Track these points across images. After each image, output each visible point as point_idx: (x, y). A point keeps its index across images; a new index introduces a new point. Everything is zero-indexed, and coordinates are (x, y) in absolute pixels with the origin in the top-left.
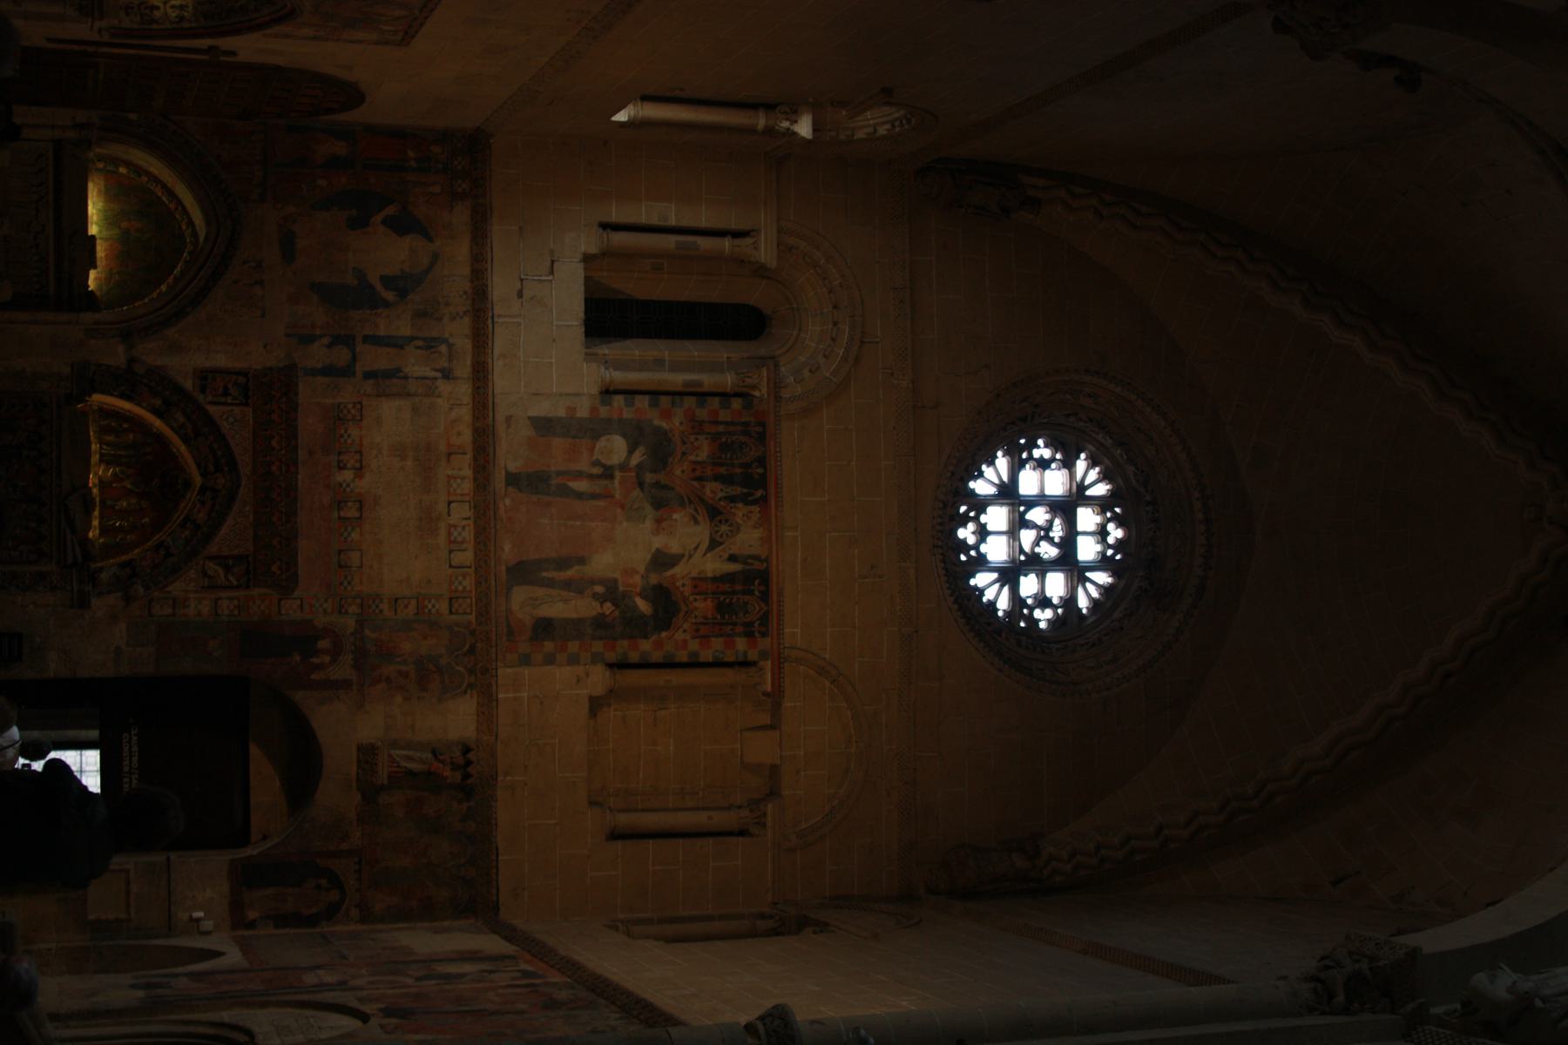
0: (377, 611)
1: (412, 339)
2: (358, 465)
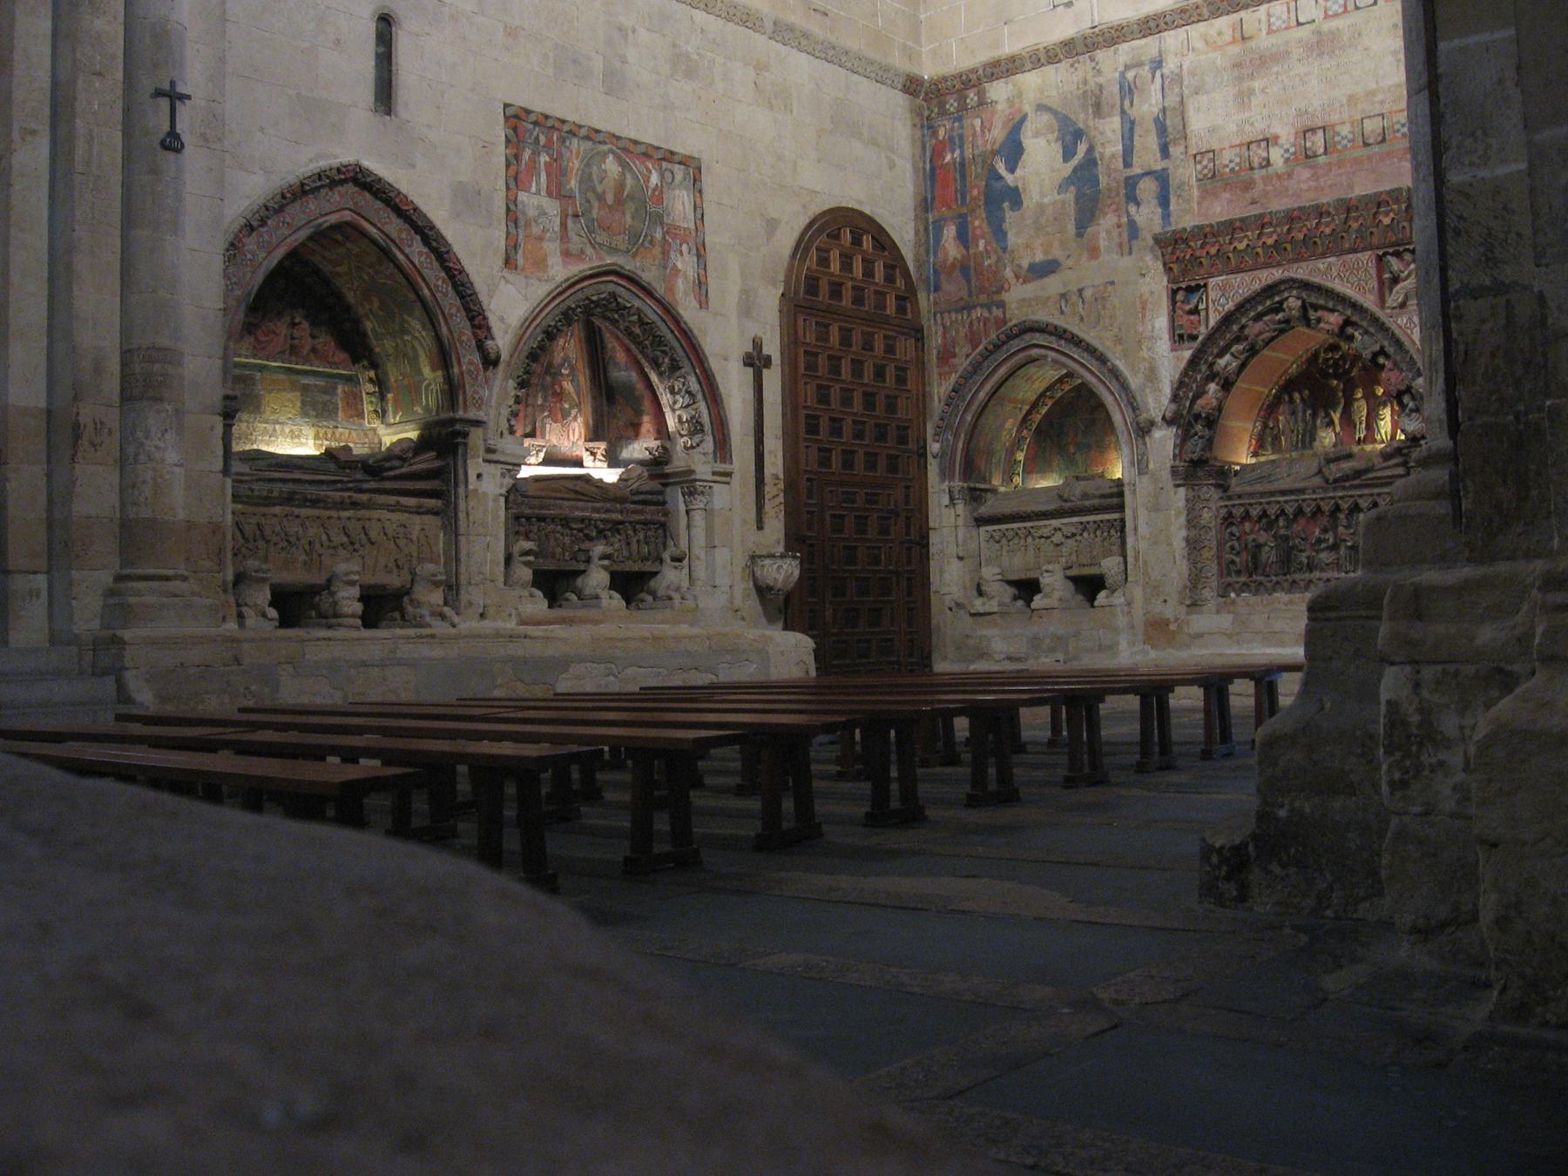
1: (1123, 112)
2: (1263, 144)
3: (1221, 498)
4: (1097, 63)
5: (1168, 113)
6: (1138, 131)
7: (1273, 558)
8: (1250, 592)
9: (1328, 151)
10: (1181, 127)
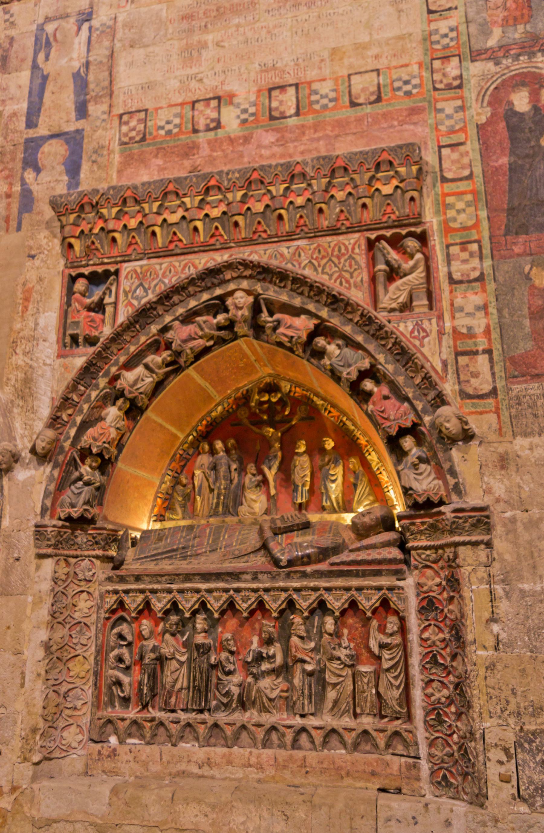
0: (454, 34)
1: (35, 66)
2: (214, 103)
3: (109, 579)
4: (12, 16)
5: (92, 68)
6: (50, 87)
7: (182, 682)
8: (142, 737)
9: (302, 111)
10: (107, 83)
